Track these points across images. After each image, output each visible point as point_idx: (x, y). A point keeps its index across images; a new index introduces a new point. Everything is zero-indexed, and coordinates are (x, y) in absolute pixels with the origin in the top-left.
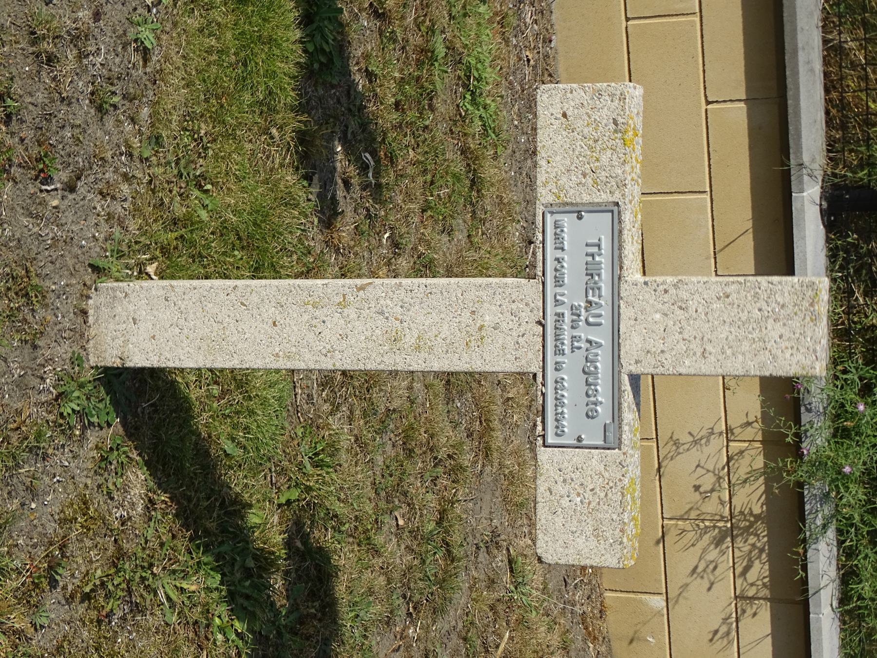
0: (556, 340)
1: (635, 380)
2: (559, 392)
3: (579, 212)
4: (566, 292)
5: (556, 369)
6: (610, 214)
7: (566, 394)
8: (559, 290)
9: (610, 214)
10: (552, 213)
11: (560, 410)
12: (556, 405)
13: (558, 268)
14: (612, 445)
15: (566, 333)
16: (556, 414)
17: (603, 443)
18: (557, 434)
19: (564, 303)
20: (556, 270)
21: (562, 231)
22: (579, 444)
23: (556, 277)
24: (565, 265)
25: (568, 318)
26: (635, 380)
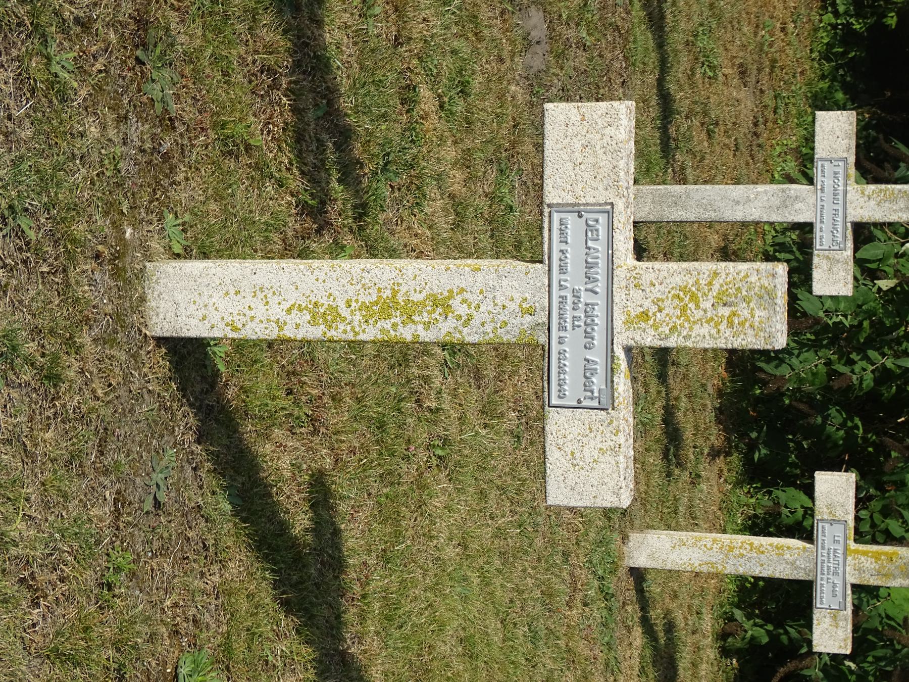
0: (560, 318)
2: (562, 361)
3: (579, 212)
4: (569, 279)
5: (560, 343)
7: (567, 363)
8: (563, 277)
10: (556, 212)
11: (562, 377)
12: (559, 373)
13: (562, 258)
14: (605, 407)
15: (568, 313)
16: (559, 380)
18: (559, 397)
19: (567, 288)
20: (561, 260)
21: (566, 227)
22: (579, 405)
23: (560, 266)
24: (568, 255)
25: (570, 300)
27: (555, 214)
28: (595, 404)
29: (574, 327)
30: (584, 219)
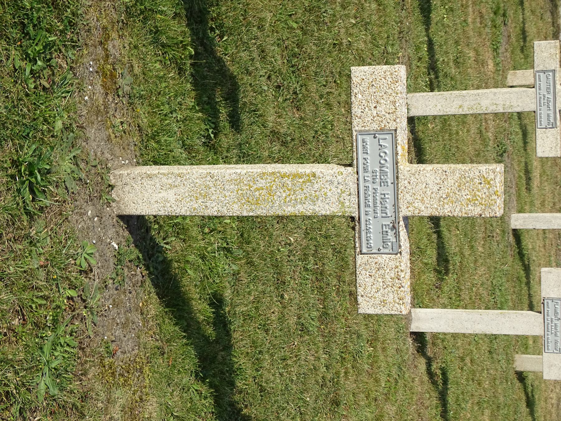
0: (365, 200)
3: (375, 134)
5: (366, 215)
8: (366, 174)
10: (360, 135)
11: (369, 235)
12: (367, 233)
13: (365, 163)
16: (367, 237)
17: (391, 251)
18: (367, 247)
20: (364, 164)
21: (367, 144)
23: (364, 168)
24: (368, 161)
27: (359, 136)
30: (377, 139)
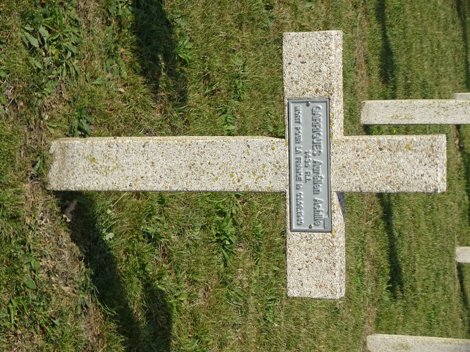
0: (297, 172)
1: (341, 195)
3: (307, 102)
5: (297, 189)
6: (325, 103)
7: (302, 202)
8: (298, 145)
9: (325, 103)
10: (293, 102)
11: (299, 211)
12: (297, 208)
18: (298, 224)
20: (296, 134)
21: (299, 113)
22: (310, 229)
23: (296, 138)
24: (301, 131)
26: (341, 195)
28: (321, 228)
29: (306, 180)
30: (310, 107)
